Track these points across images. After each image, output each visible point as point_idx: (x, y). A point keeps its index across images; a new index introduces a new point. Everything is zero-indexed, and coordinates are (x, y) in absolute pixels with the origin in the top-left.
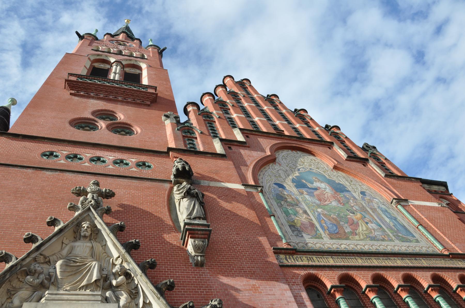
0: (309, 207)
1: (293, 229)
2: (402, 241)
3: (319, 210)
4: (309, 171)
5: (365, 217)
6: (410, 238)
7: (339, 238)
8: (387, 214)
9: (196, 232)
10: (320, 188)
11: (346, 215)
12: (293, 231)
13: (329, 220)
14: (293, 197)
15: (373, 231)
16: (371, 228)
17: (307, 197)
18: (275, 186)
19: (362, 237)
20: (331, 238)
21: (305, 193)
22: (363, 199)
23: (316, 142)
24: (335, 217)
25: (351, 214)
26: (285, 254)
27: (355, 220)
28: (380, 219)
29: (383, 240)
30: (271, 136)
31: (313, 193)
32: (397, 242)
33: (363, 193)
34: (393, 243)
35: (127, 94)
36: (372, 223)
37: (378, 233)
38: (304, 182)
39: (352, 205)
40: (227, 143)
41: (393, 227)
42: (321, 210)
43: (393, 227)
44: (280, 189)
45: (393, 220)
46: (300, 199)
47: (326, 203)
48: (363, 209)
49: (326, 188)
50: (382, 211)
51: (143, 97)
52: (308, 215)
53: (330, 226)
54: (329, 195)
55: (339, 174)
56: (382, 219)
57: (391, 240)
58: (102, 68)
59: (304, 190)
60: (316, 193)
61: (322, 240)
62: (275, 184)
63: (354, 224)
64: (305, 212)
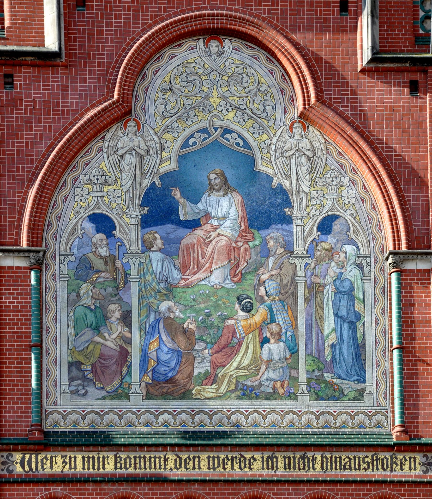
0: (142, 298)
1: (75, 372)
2: (319, 398)
4: (215, 143)
5: (273, 321)
7: (167, 396)
8: (344, 303)
12: (71, 379)
14: (118, 263)
15: (264, 367)
17: (156, 257)
19: (223, 389)
20: (149, 396)
21: (159, 242)
22: (311, 251)
25: (241, 314)
26: (24, 451)
28: (309, 327)
31: (179, 240)
32: (304, 401)
33: (326, 226)
36: (279, 340)
37: (272, 375)
39: (264, 277)
41: (328, 351)
43: (328, 351)
45: (346, 326)
46: (134, 272)
49: (224, 218)
50: (338, 292)
52: (129, 325)
54: (223, 241)
56: (314, 325)
57: (292, 396)
63: (228, 347)
64: (126, 318)
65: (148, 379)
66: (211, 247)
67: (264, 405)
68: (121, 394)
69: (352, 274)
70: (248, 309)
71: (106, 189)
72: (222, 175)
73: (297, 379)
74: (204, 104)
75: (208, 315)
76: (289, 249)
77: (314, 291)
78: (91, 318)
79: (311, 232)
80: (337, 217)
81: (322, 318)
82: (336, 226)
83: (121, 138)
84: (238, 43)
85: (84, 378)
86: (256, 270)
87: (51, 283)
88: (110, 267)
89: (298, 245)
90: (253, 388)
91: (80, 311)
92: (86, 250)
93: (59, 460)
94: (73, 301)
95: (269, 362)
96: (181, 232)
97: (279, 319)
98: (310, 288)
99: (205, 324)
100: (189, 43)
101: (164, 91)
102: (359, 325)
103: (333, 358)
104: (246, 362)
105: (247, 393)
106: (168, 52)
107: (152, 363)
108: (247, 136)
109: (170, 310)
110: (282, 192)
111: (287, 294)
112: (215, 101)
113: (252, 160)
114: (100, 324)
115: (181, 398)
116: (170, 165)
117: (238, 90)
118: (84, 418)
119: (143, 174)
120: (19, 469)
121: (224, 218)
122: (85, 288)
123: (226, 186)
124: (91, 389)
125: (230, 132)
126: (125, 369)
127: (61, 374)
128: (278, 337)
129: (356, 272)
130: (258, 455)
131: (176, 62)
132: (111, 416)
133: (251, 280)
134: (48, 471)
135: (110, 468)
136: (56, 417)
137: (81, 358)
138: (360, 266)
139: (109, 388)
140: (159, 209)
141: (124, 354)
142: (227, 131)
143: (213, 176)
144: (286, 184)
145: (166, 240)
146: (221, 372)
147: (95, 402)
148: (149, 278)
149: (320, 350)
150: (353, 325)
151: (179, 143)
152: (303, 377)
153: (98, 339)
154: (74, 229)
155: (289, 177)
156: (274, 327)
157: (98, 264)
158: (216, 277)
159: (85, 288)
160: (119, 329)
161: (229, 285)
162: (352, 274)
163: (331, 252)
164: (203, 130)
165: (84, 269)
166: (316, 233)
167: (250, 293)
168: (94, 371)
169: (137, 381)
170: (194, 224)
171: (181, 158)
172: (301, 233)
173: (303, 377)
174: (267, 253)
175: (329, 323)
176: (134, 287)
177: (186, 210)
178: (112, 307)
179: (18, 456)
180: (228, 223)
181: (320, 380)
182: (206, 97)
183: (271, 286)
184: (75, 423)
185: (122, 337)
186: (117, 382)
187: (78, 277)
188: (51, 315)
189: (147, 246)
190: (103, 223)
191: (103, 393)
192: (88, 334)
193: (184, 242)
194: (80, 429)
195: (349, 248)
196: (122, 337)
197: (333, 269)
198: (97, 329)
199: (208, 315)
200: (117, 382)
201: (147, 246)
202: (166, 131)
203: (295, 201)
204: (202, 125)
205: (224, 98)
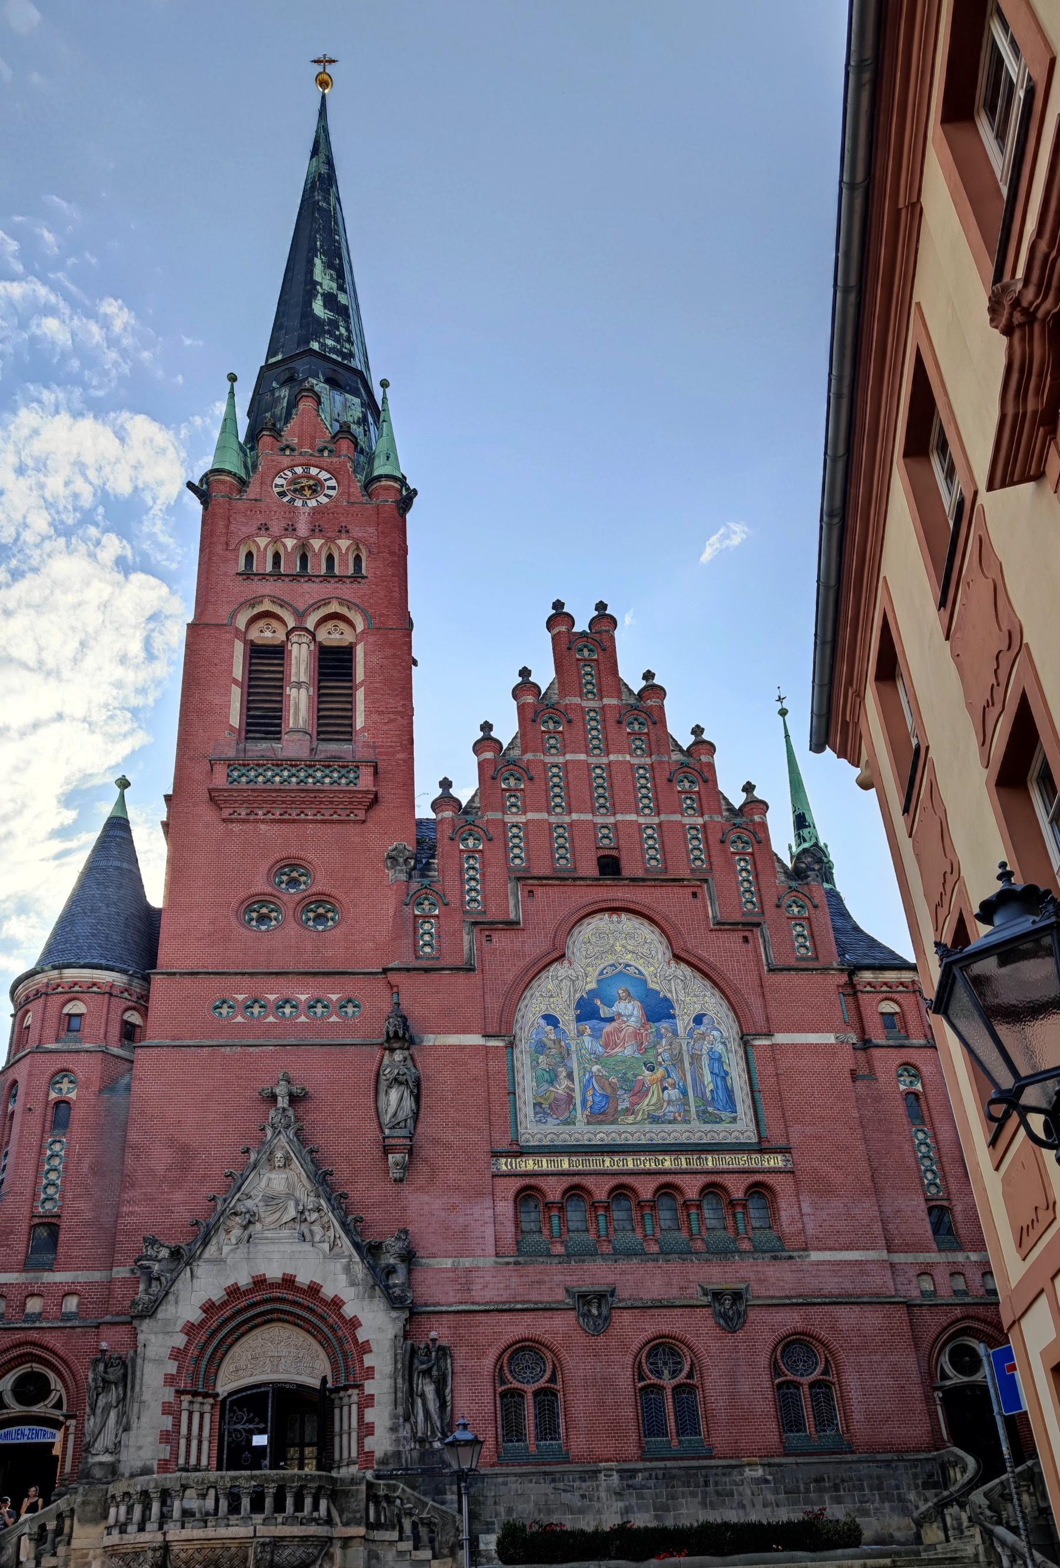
0: (579, 1064)
1: (538, 1109)
3: (595, 1068)
4: (621, 972)
5: (669, 1076)
6: (724, 1115)
7: (601, 1123)
8: (716, 1065)
10: (620, 1015)
11: (635, 1076)
12: (536, 1114)
14: (563, 1043)
15: (665, 1104)
16: (666, 1097)
17: (587, 1039)
18: (542, 1022)
19: (639, 1118)
20: (589, 1123)
21: (589, 1031)
22: (690, 1035)
26: (506, 1157)
28: (694, 1080)
30: (578, 883)
31: (601, 1029)
32: (696, 1124)
33: (698, 1020)
34: (686, 1127)
35: (321, 802)
36: (675, 1088)
37: (672, 1109)
39: (660, 1051)
41: (708, 1094)
43: (708, 1094)
45: (719, 1079)
46: (573, 1048)
49: (630, 1016)
50: (711, 1059)
51: (351, 803)
52: (573, 1081)
53: (597, 1099)
54: (631, 1029)
55: (679, 973)
56: (697, 1081)
57: (687, 1121)
58: (270, 642)
60: (609, 1028)
61: (572, 1127)
63: (640, 1092)
64: (570, 1076)
67: (669, 1127)
68: (570, 1122)
70: (652, 1069)
73: (689, 1111)
74: (612, 950)
75: (625, 1074)
76: (675, 1033)
77: (695, 1058)
78: (547, 1076)
79: (688, 1024)
80: (705, 1015)
81: (702, 1075)
82: (705, 1020)
83: (559, 970)
84: (630, 916)
85: (545, 1113)
86: (654, 1046)
87: (520, 1055)
88: (557, 1046)
89: (680, 1031)
90: (659, 1118)
91: (539, 1072)
92: (541, 1036)
93: (531, 1162)
95: (669, 1102)
96: (602, 1024)
97: (673, 1075)
98: (692, 1057)
99: (624, 1079)
100: (599, 916)
101: (585, 943)
102: (728, 1079)
103: (713, 1098)
104: (654, 1101)
105: (655, 1120)
106: (586, 921)
107: (590, 1103)
109: (599, 1071)
110: (666, 999)
111: (677, 1060)
112: (618, 948)
113: (645, 982)
115: (612, 1123)
116: (592, 986)
117: (631, 942)
118: (546, 1137)
119: (575, 991)
120: (504, 1168)
121: (630, 1016)
122: (541, 1058)
123: (629, 996)
125: (630, 966)
127: (529, 1110)
128: (674, 1086)
129: (721, 1046)
130: (667, 1158)
131: (591, 927)
132: (564, 1135)
133: (652, 1052)
134: (523, 1169)
135: (566, 1166)
136: (527, 1136)
137: (542, 1101)
138: (724, 1043)
140: (586, 1011)
141: (570, 1098)
143: (620, 992)
144: (669, 995)
145: (592, 1029)
146: (637, 1108)
148: (583, 1052)
149: (703, 1094)
150: (724, 1079)
151: (597, 973)
152: (693, 1109)
153: (552, 1089)
154: (533, 1023)
155: (670, 991)
156: (670, 1080)
157: (549, 1044)
158: (628, 1051)
160: (566, 1082)
161: (637, 1055)
162: (719, 1048)
163: (703, 1036)
164: (612, 965)
165: (541, 1047)
166: (692, 1024)
168: (550, 1107)
169: (580, 1115)
170: (611, 1020)
171: (599, 981)
172: (683, 1023)
173: (693, 1109)
174: (660, 1036)
175: (708, 1078)
176: (574, 1056)
178: (560, 1069)
179: (503, 1160)
180: (633, 1019)
181: (705, 1112)
182: (612, 946)
183: (666, 1056)
184: (540, 1140)
185: (568, 1087)
186: (566, 1115)
187: (536, 1052)
188: (520, 1075)
189: (580, 1033)
190: (551, 1020)
191: (558, 1121)
192: (545, 1086)
193: (605, 1030)
194: (544, 1143)
195: (715, 1033)
196: (568, 1087)
197: (706, 1046)
198: (551, 1083)
199: (625, 1074)
201: (580, 1033)
202: (588, 965)
203: (676, 1005)
205: (624, 947)
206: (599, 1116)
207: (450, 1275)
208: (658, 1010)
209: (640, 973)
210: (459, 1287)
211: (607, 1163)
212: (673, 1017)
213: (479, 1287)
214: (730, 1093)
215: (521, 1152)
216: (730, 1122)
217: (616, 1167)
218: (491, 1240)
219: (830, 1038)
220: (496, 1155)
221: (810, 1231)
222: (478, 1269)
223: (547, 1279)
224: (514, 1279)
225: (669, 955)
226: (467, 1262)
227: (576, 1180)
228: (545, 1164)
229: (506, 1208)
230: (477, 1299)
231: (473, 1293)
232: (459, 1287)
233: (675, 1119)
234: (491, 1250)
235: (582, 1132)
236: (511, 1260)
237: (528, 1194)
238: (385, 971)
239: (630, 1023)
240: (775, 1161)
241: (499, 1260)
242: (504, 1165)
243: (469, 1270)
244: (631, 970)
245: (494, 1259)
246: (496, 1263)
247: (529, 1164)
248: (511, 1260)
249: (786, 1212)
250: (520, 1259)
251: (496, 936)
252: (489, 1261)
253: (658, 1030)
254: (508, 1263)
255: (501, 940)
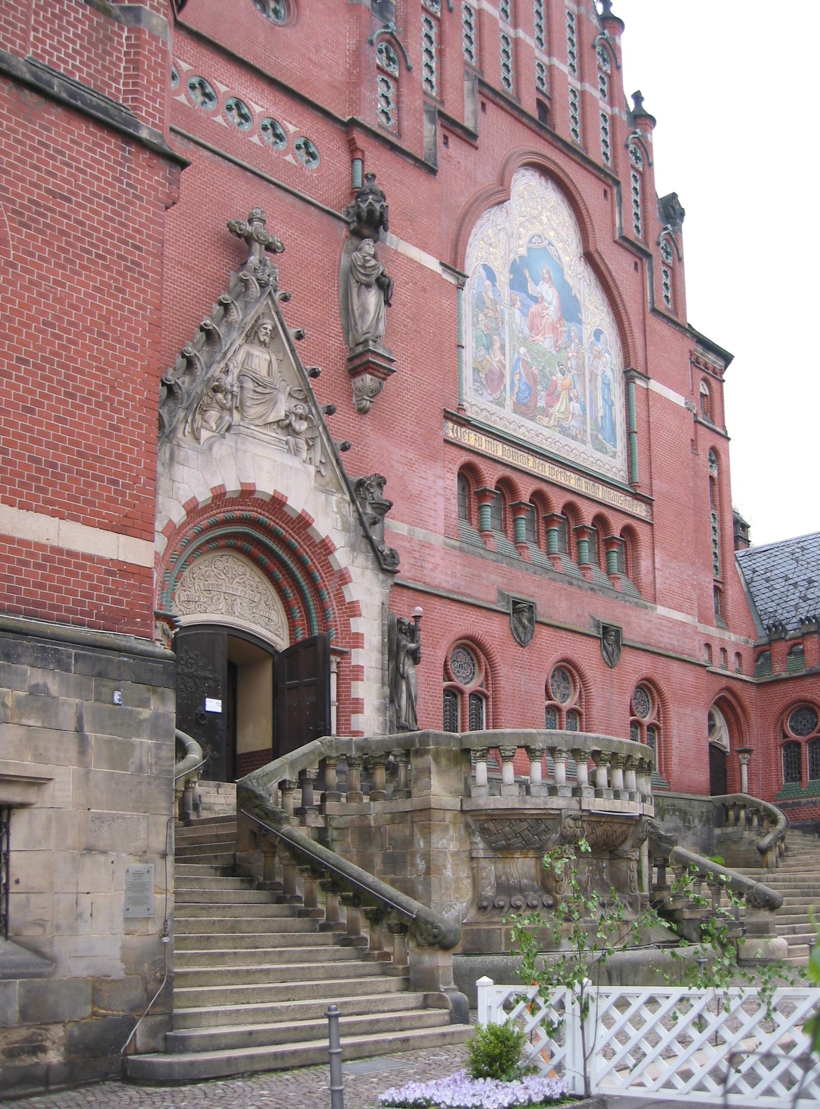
3: (522, 350)
6: (609, 446)
7: (524, 415)
8: (606, 391)
9: (378, 368)
11: (552, 374)
12: (475, 380)
13: (527, 375)
17: (517, 313)
20: (515, 411)
21: (519, 303)
23: (590, 168)
24: (536, 371)
25: (560, 375)
27: (559, 388)
29: (574, 438)
31: (529, 307)
32: (589, 448)
36: (577, 402)
38: (527, 275)
39: (570, 355)
40: (446, 123)
42: (525, 350)
44: (488, 283)
46: (506, 318)
47: (538, 337)
48: (581, 369)
52: (504, 356)
53: (523, 387)
54: (550, 321)
57: (584, 442)
59: (519, 296)
60: (534, 308)
61: (501, 409)
62: (486, 268)
63: (553, 396)
65: (514, 398)
66: (544, 320)
68: (500, 403)
69: (609, 373)
71: (492, 250)
72: (548, 272)
74: (538, 218)
76: (581, 339)
85: (481, 383)
86: (566, 348)
94: (476, 324)
96: (528, 301)
97: (578, 387)
104: (562, 410)
105: (564, 431)
107: (516, 389)
108: (560, 252)
113: (561, 270)
114: (489, 348)
116: (523, 251)
120: (451, 434)
121: (550, 303)
124: (485, 393)
126: (502, 386)
130: (573, 475)
138: (612, 369)
139: (494, 395)
141: (502, 376)
142: (550, 244)
146: (551, 410)
147: (486, 402)
151: (528, 238)
153: (488, 357)
159: (481, 317)
164: (539, 236)
165: (480, 304)
167: (564, 362)
171: (529, 250)
172: (587, 332)
177: (531, 287)
179: (450, 425)
181: (597, 438)
189: (513, 304)
192: (483, 352)
195: (607, 355)
196: (500, 362)
200: (498, 394)
201: (513, 304)
203: (583, 310)
204: (539, 233)
205: (549, 220)
206: (525, 409)
207: (407, 544)
208: (570, 310)
209: (559, 258)
210: (412, 561)
211: (531, 464)
212: (580, 322)
213: (430, 566)
214: (613, 425)
215: (465, 423)
216: (612, 457)
217: (536, 470)
218: (442, 514)
219: (679, 400)
220: (448, 416)
221: (658, 586)
222: (430, 546)
223: (484, 575)
224: (459, 567)
225: (580, 250)
226: (420, 533)
227: (508, 472)
228: (482, 444)
229: (453, 482)
230: (428, 580)
231: (425, 572)
232: (412, 561)
233: (576, 436)
234: (441, 526)
235: (506, 419)
236: (457, 544)
237: (468, 475)
238: (353, 123)
239: (551, 313)
240: (640, 510)
241: (448, 540)
242: (452, 431)
243: (424, 545)
244: (551, 250)
245: (443, 537)
246: (446, 544)
247: (470, 439)
248: (457, 544)
249: (645, 564)
250: (464, 545)
251: (452, 140)
252: (437, 539)
253: (569, 331)
254: (454, 547)
255: (456, 148)
